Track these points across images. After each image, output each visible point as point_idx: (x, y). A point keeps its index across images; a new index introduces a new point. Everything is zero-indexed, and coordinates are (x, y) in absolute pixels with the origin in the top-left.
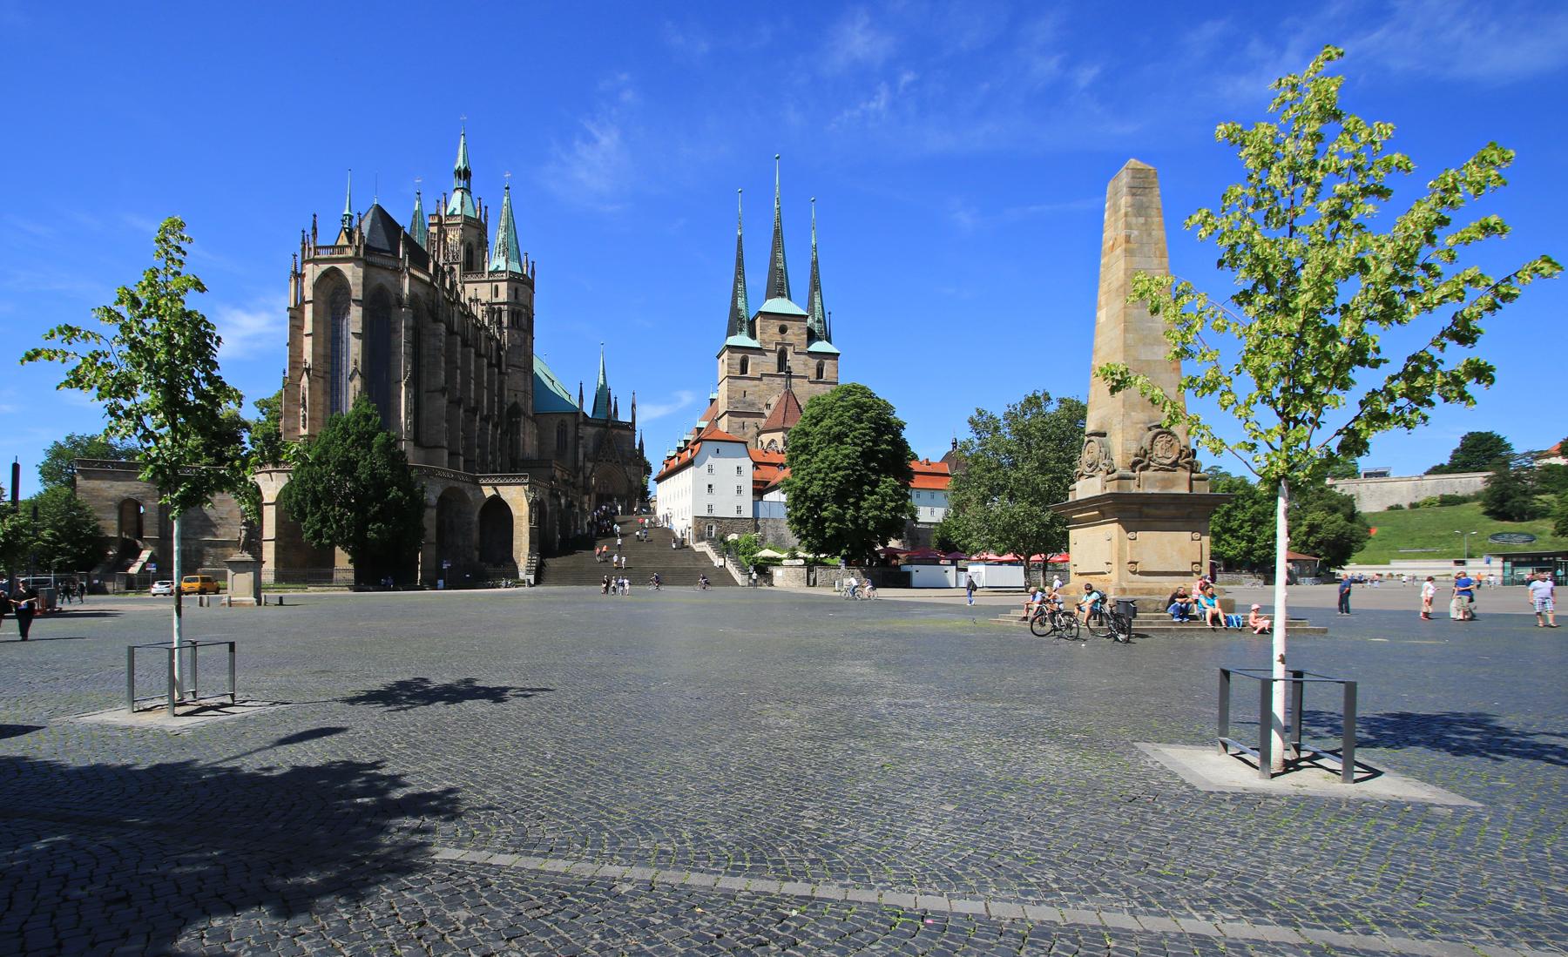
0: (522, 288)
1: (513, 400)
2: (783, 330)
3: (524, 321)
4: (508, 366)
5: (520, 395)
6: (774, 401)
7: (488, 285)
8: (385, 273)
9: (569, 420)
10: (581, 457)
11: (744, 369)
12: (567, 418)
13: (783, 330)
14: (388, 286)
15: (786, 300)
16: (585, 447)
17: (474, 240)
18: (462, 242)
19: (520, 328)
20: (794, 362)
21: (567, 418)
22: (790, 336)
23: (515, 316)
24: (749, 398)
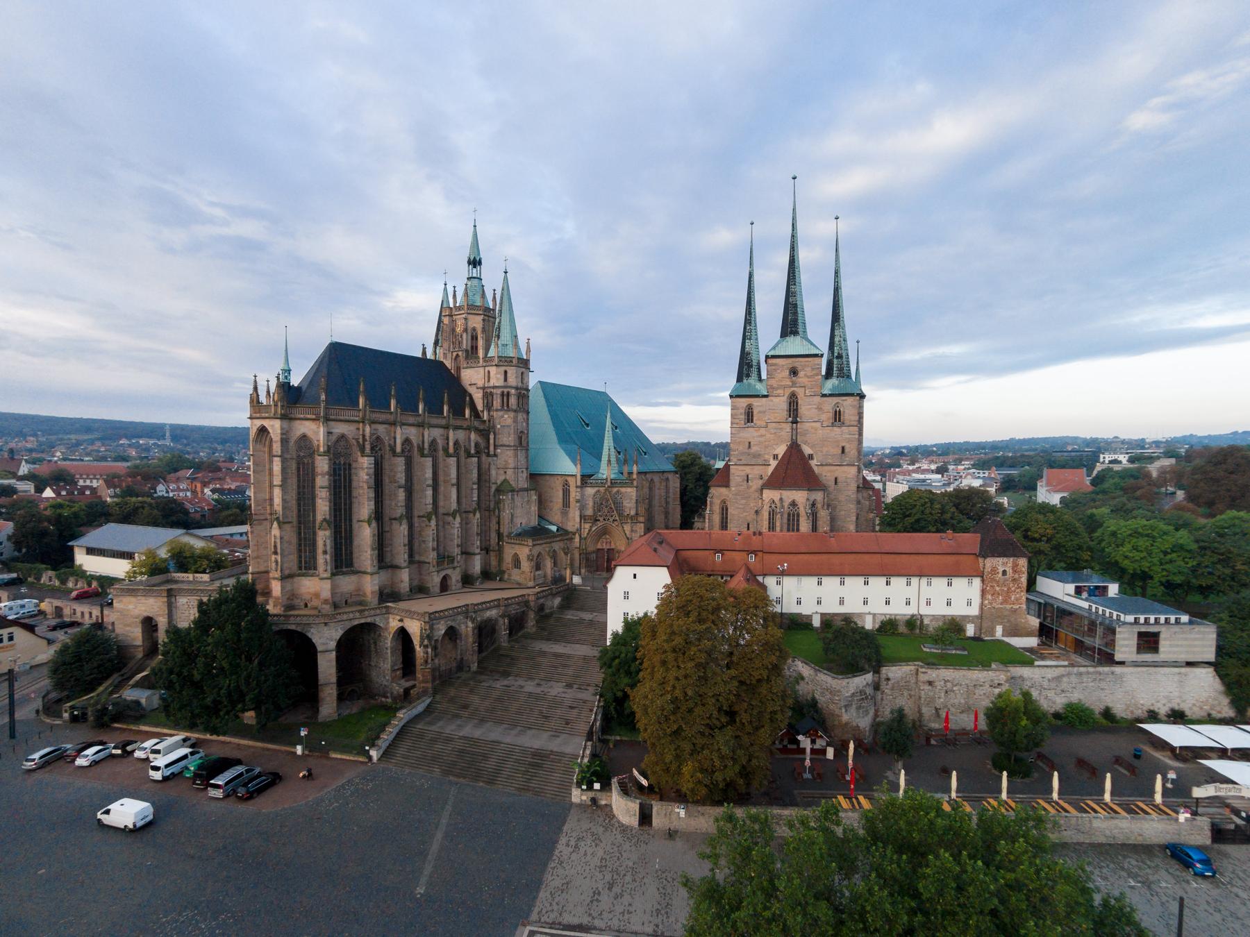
0: (512, 372)
1: (502, 478)
2: (794, 372)
3: (513, 401)
4: (495, 447)
5: (510, 472)
6: (781, 450)
7: (481, 370)
8: (308, 423)
9: (571, 481)
10: (578, 519)
11: (749, 416)
12: (569, 479)
13: (794, 372)
14: (310, 434)
15: (798, 339)
16: (582, 508)
17: (479, 327)
18: (466, 330)
19: (509, 409)
20: (807, 409)
21: (569, 479)
22: (802, 378)
23: (505, 396)
24: (754, 449)
